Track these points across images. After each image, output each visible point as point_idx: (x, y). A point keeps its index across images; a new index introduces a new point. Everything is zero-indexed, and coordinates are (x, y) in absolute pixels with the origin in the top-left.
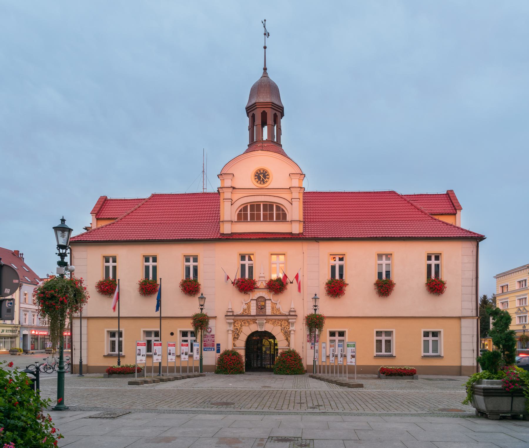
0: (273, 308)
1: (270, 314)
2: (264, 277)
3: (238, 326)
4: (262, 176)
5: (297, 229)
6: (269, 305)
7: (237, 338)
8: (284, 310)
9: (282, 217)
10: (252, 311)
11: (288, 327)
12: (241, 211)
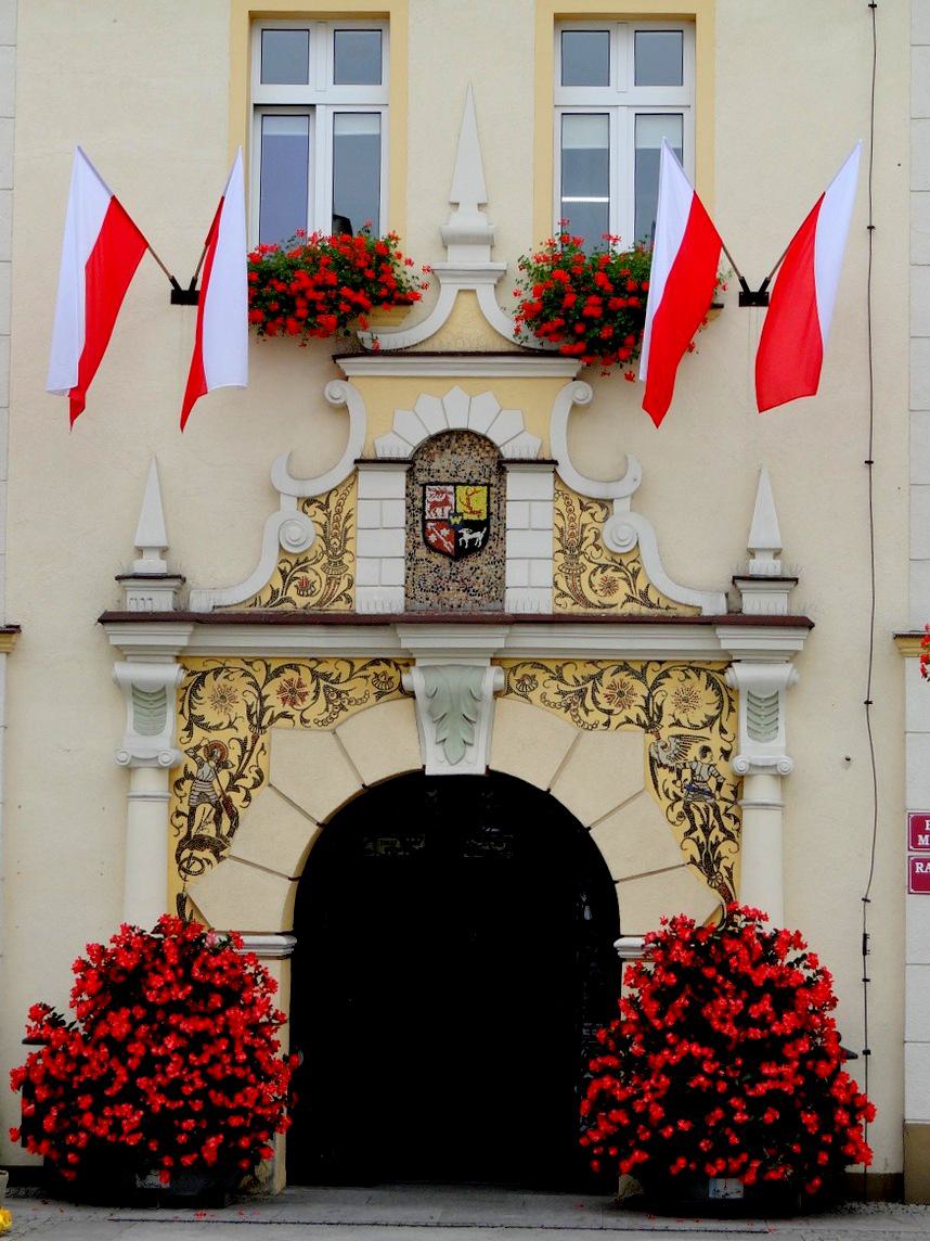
1: (544, 604)
2: (488, 241)
3: (227, 722)
6: (529, 511)
7: (218, 847)
8: (688, 573)
10: (362, 571)
11: (716, 742)
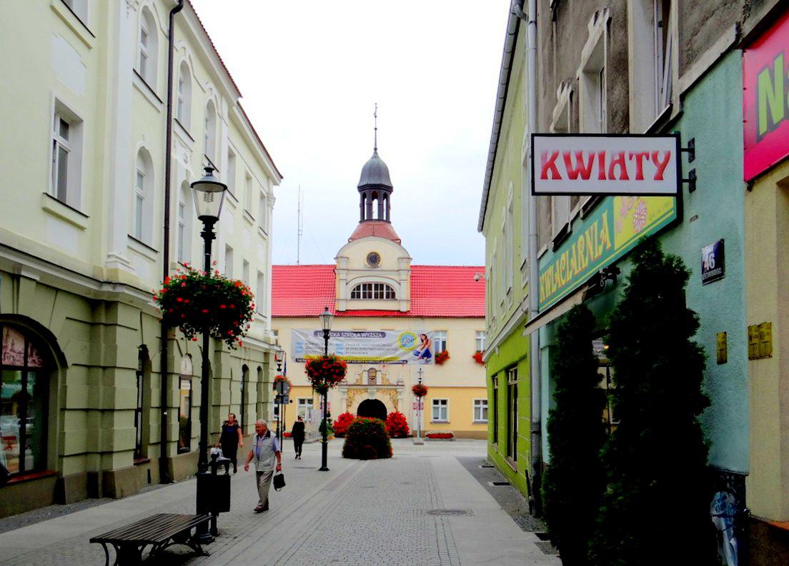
0: (383, 378)
1: (380, 384)
4: (374, 259)
5: (404, 307)
6: (379, 376)
9: (391, 295)
12: (354, 290)
